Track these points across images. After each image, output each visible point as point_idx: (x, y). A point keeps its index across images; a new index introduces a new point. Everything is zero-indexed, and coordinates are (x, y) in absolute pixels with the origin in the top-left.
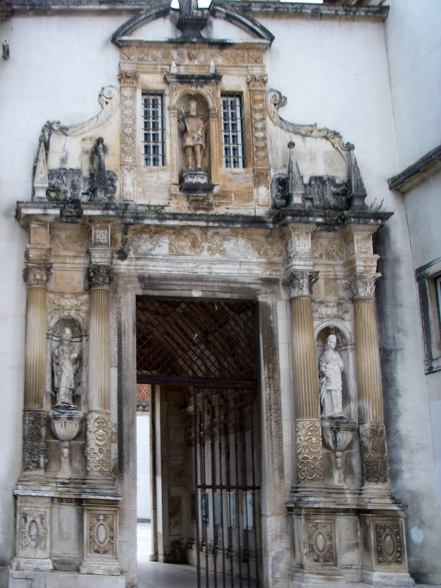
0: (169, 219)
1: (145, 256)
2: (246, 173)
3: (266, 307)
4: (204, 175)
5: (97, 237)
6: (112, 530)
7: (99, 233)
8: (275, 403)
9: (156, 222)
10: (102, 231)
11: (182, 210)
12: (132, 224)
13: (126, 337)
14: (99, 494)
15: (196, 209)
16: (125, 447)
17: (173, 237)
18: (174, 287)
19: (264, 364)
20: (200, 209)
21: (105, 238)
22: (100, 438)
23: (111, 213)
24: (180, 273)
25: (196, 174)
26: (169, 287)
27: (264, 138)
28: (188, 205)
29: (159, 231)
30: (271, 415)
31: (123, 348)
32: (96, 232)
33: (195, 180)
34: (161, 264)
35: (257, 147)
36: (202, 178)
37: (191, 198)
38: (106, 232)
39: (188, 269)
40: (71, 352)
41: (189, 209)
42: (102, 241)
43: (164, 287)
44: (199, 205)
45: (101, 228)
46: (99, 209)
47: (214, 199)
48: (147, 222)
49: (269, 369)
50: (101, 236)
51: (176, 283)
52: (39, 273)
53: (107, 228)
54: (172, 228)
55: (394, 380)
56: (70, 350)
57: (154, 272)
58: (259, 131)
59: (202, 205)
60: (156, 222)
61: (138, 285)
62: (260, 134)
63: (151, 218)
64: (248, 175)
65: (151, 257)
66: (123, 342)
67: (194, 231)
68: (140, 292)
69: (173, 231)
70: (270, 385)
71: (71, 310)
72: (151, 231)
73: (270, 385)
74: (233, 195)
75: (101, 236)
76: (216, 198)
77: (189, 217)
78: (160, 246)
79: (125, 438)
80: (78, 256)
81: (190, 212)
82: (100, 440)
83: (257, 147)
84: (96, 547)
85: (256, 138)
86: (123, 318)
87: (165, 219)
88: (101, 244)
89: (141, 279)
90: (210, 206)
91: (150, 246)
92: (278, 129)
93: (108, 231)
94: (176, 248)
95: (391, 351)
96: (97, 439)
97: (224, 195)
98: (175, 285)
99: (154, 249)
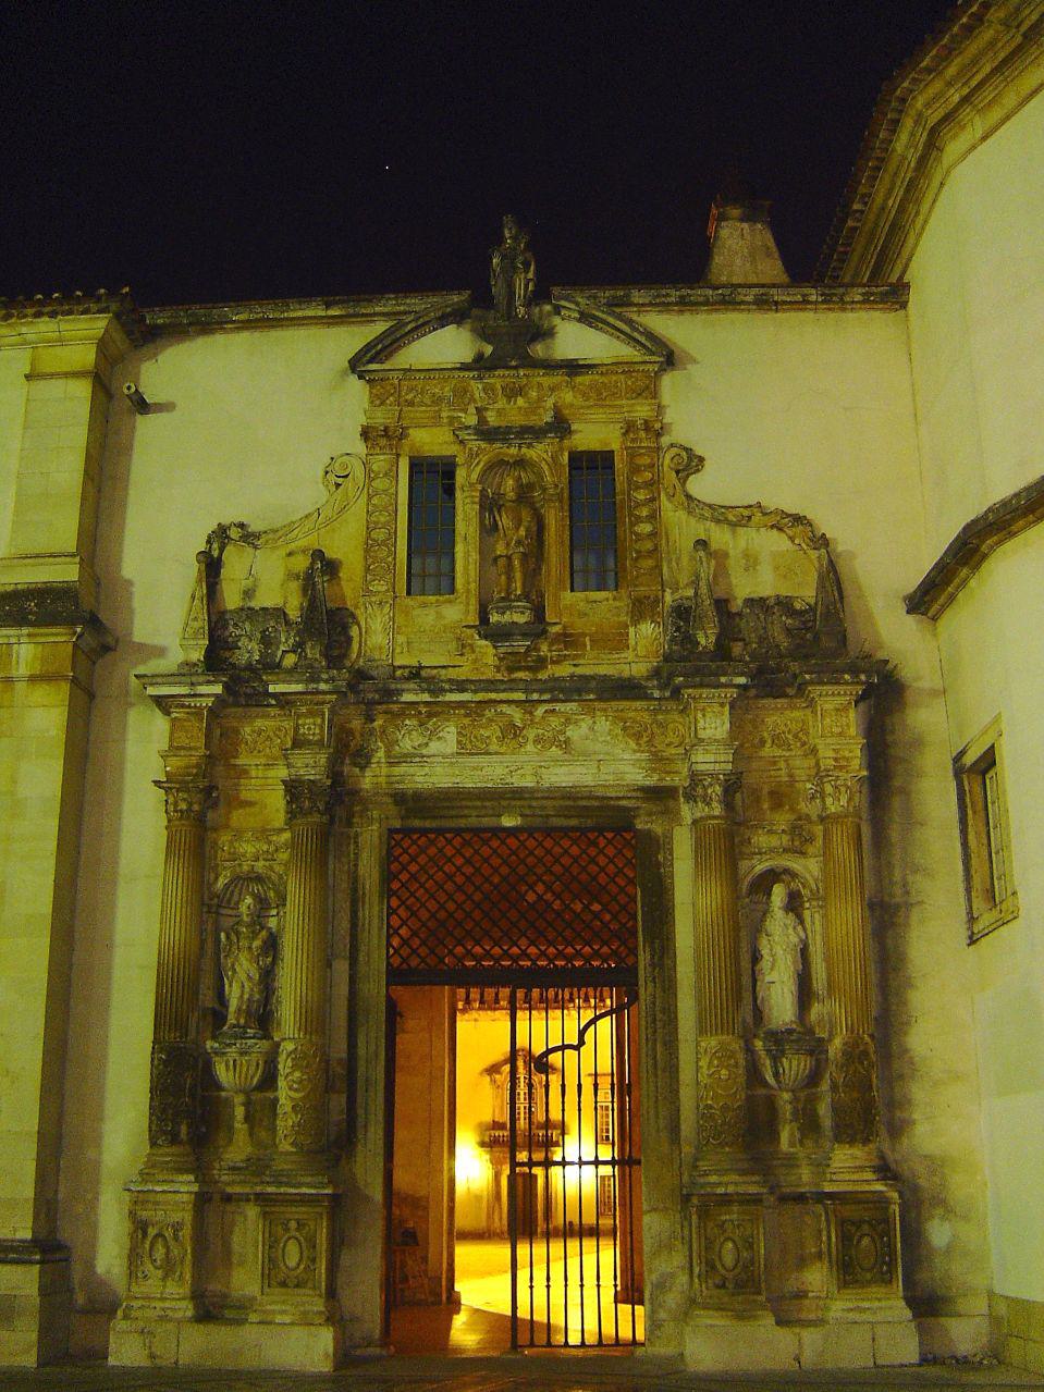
0: (451, 691)
1: (406, 758)
2: (615, 599)
3: (648, 834)
4: (524, 607)
5: (302, 731)
6: (314, 1247)
7: (303, 726)
8: (664, 1008)
9: (426, 697)
10: (311, 720)
11: (482, 674)
12: (380, 704)
13: (367, 906)
14: (288, 1184)
15: (511, 670)
16: (360, 1100)
17: (467, 721)
18: (466, 812)
19: (644, 942)
20: (519, 669)
21: (317, 731)
22: (295, 1086)
23: (323, 686)
24: (479, 785)
25: (510, 608)
26: (454, 813)
27: (654, 534)
28: (497, 663)
29: (435, 711)
30: (655, 1032)
31: (360, 924)
32: (300, 722)
33: (507, 618)
34: (439, 770)
35: (638, 552)
36: (523, 613)
37: (502, 650)
38: (319, 721)
39: (494, 778)
40: (255, 935)
41: (498, 669)
42: (311, 737)
43: (445, 812)
44: (520, 661)
45: (305, 716)
46: (298, 682)
47: (550, 651)
48: (407, 697)
49: (653, 950)
50: (309, 729)
51: (469, 804)
52: (184, 799)
53: (323, 714)
54: (461, 704)
55: (902, 958)
56: (253, 932)
57: (425, 786)
58: (642, 522)
59: (526, 661)
60: (426, 697)
61: (393, 810)
62: (645, 528)
63: (415, 692)
64: (618, 604)
65: (417, 759)
66: (360, 914)
67: (504, 708)
68: (397, 824)
69: (463, 711)
70: (654, 978)
71: (257, 860)
72: (420, 713)
73: (654, 978)
74: (587, 638)
75: (309, 729)
76: (554, 648)
77: (490, 686)
78: (439, 738)
79: (361, 1084)
80: (272, 765)
81: (499, 676)
82: (296, 1090)
83: (638, 552)
84: (281, 1277)
85: (637, 534)
86: (361, 871)
87: (443, 691)
88: (310, 743)
89: (400, 798)
90: (542, 663)
91: (422, 740)
92: (682, 514)
93: (323, 719)
94: (471, 742)
95: (898, 907)
96: (290, 1088)
97: (568, 640)
98: (467, 807)
99: (427, 744)
